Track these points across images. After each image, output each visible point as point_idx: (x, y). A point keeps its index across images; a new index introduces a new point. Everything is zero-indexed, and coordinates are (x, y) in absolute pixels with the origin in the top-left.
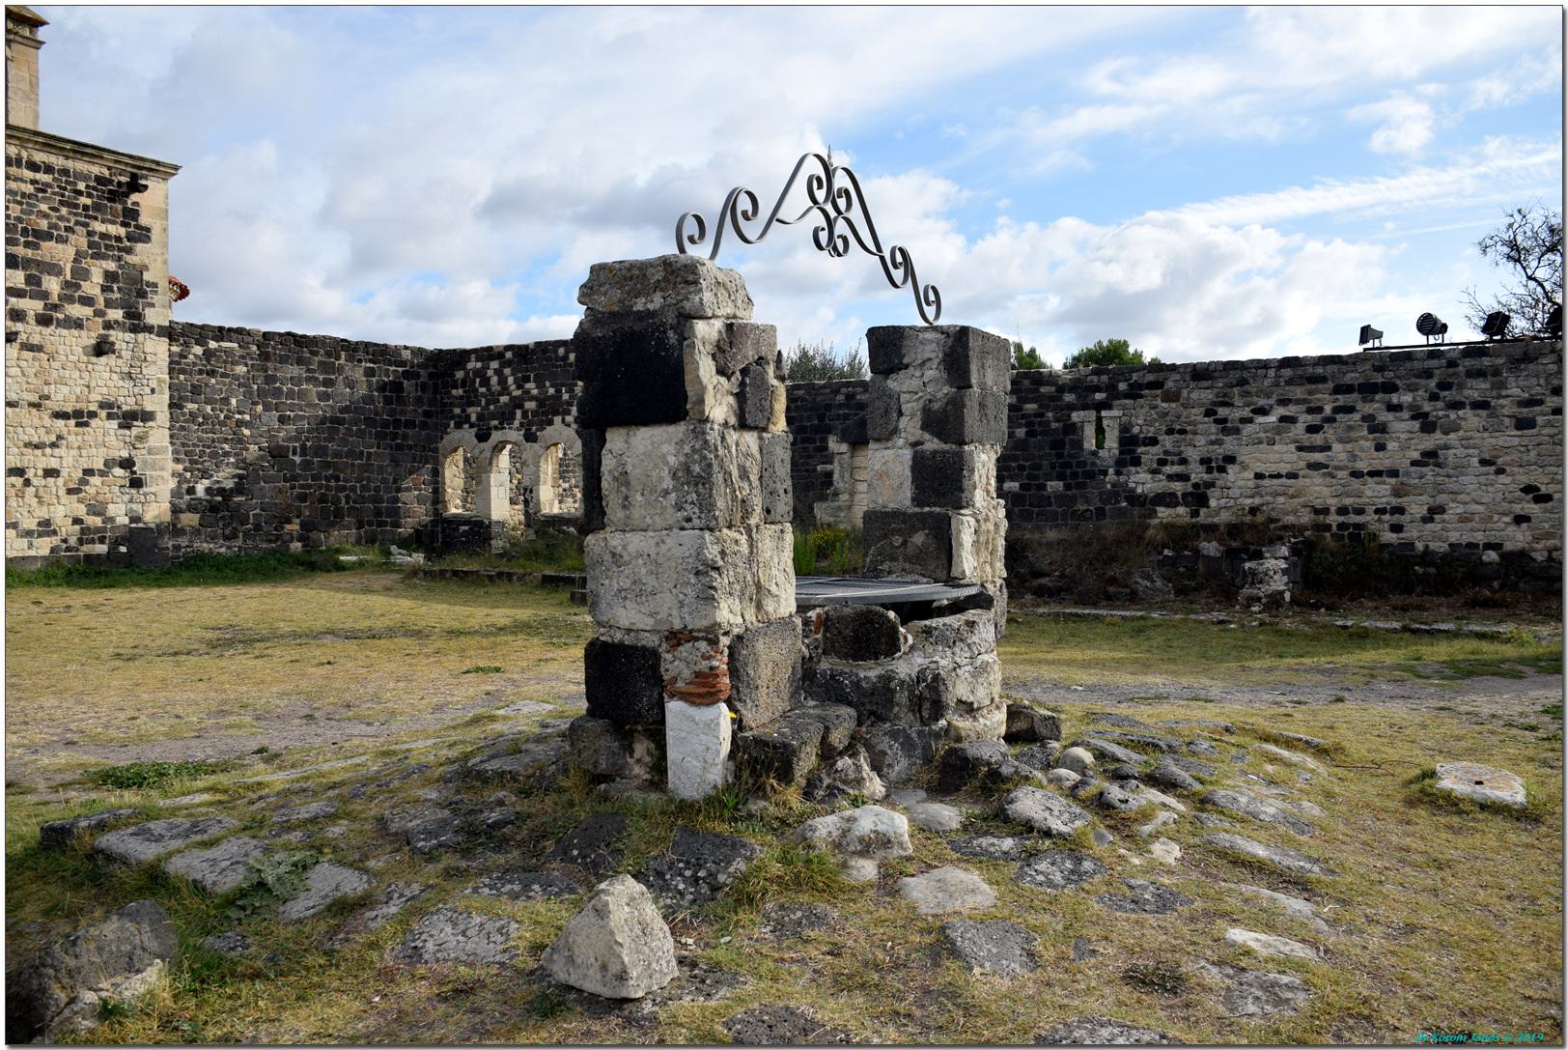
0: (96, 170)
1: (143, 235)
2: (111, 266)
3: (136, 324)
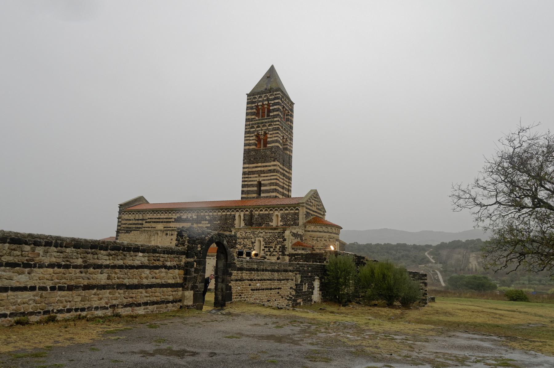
0: (278, 231)
1: (285, 240)
2: (280, 245)
3: (284, 254)
